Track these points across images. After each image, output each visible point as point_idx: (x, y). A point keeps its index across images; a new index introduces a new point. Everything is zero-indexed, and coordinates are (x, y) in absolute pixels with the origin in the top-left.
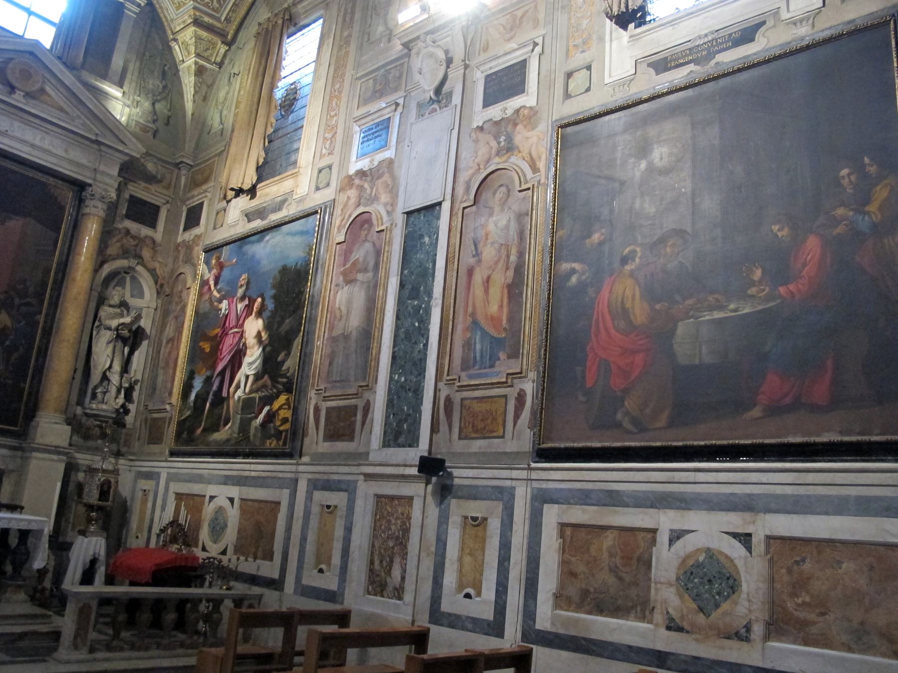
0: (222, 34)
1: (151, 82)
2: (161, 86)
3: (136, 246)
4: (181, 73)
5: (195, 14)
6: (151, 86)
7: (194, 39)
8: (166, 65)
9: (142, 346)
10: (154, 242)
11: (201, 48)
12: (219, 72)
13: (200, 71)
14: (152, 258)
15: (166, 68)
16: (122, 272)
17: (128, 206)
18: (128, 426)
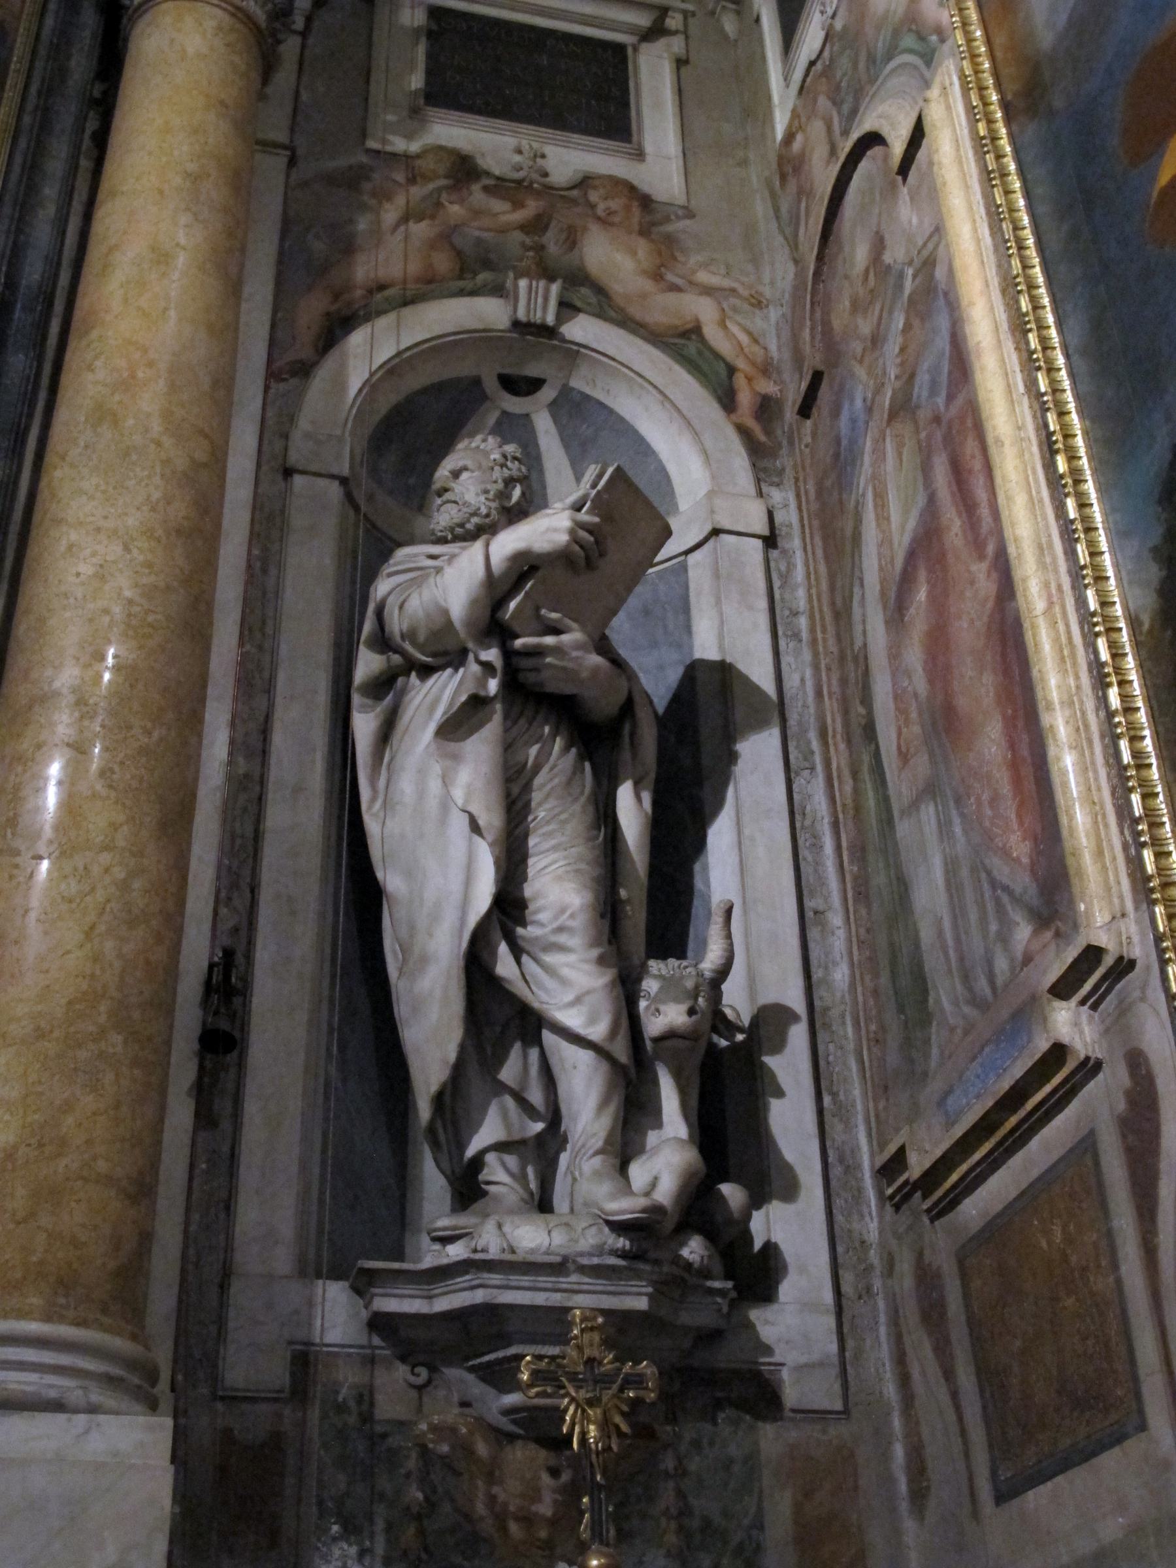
3: (537, 225)
9: (740, 768)
10: (646, 202)
14: (657, 276)
16: (491, 384)
17: (430, 56)
18: (791, 1395)
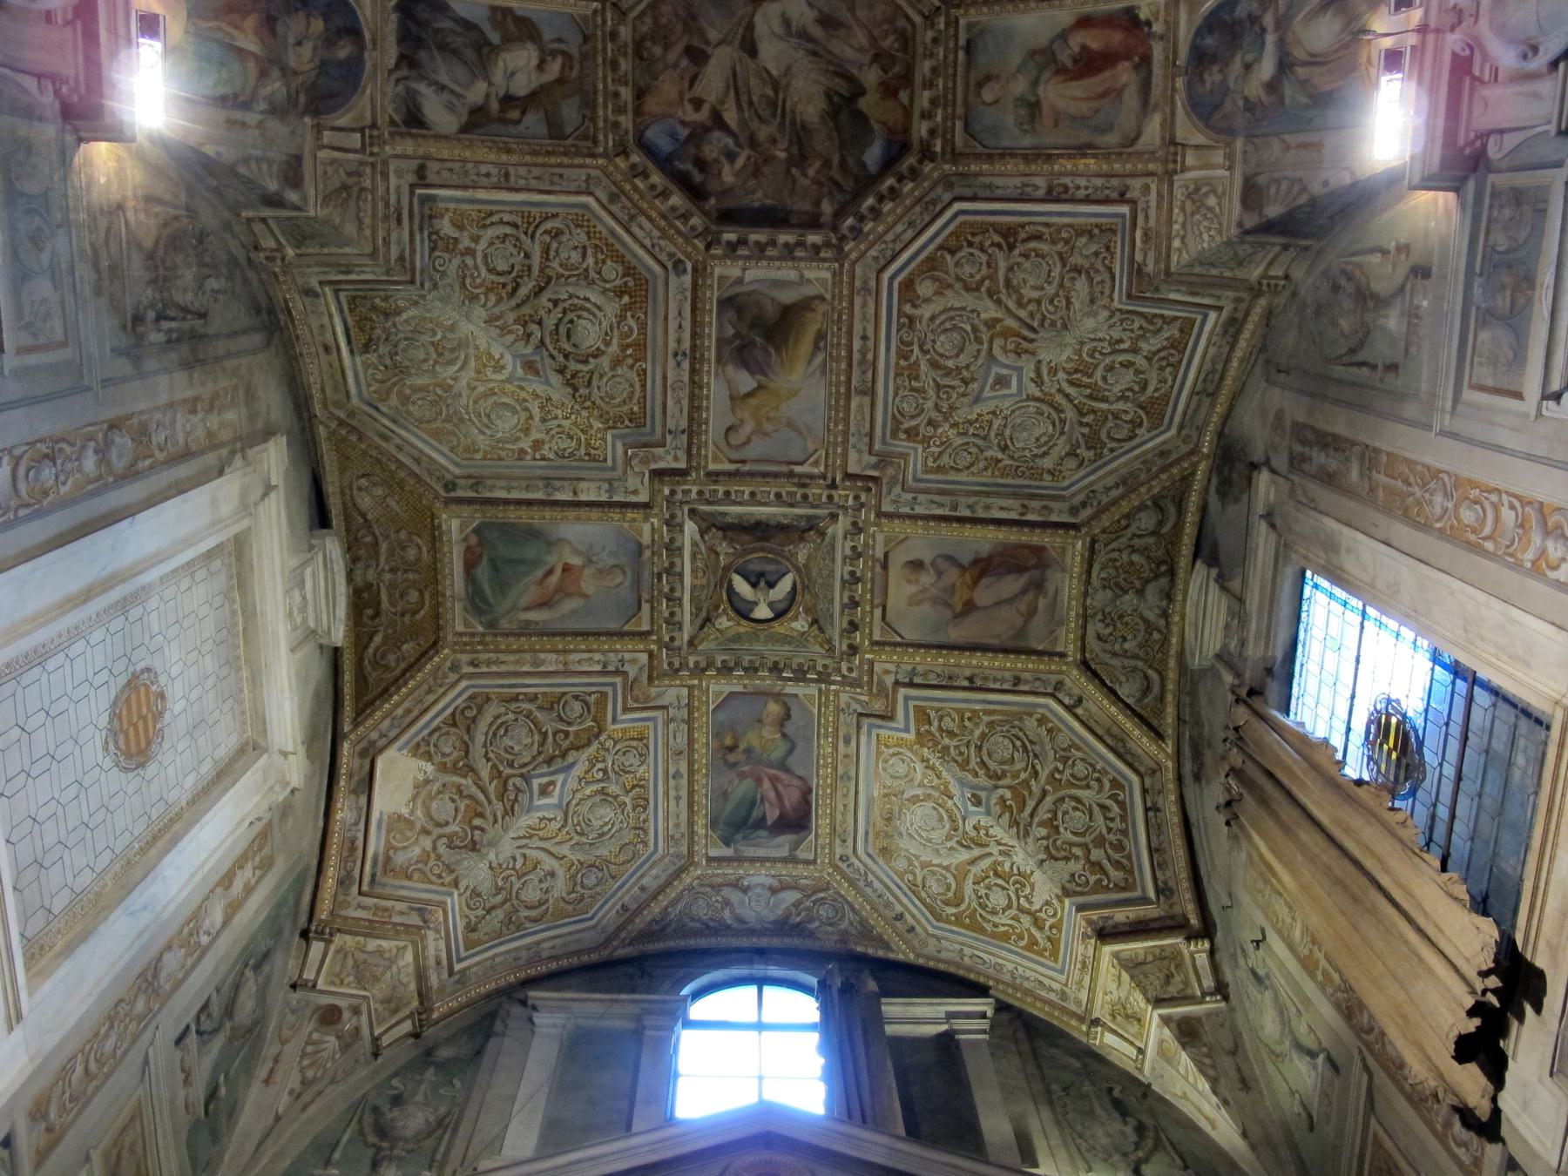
0: (1171, 925)
1: (1100, 1133)
2: (1129, 1130)
4: (1155, 1087)
5: (1090, 922)
6: (1105, 1141)
7: (1126, 977)
8: (1110, 1090)
11: (1156, 980)
12: (1232, 1009)
13: (1187, 1032)
15: (1116, 1093)
